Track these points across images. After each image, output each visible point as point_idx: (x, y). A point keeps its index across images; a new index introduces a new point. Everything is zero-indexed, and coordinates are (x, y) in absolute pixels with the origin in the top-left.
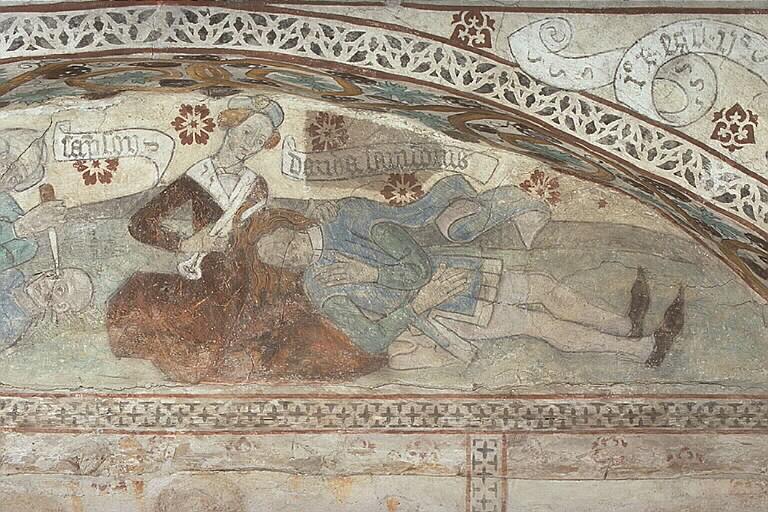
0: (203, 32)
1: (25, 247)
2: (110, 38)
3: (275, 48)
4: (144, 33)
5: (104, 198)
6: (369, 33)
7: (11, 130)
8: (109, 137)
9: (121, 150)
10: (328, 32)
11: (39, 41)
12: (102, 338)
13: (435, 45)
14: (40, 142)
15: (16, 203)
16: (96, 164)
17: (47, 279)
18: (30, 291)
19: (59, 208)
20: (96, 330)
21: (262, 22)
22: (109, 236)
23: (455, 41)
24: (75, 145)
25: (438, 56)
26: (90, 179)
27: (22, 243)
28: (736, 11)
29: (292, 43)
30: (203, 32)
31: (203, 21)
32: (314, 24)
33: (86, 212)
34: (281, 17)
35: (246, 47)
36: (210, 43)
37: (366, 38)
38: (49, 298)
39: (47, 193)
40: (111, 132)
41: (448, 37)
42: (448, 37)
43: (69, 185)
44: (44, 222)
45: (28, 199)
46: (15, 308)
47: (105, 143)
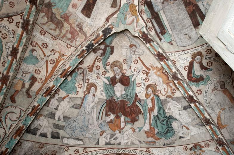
0: (120, 151)
2: (110, 152)
3: (127, 153)
4: (113, 152)
6: (137, 151)
10: (133, 151)
11: (102, 153)
13: (145, 152)
21: (126, 150)
23: (146, 151)
25: (145, 153)
28: (175, 146)
29: (129, 152)
30: (120, 151)
31: (120, 150)
32: (131, 150)
34: (128, 149)
35: (124, 153)
36: (120, 153)
37: (137, 151)
41: (146, 151)
42: (146, 151)
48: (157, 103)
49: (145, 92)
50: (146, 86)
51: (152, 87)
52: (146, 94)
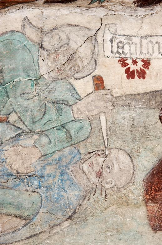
1: (81, 128)
5: (141, 91)
7: (71, 25)
8: (144, 41)
9: (153, 53)
12: (141, 213)
14: (93, 38)
15: (74, 89)
16: (135, 62)
17: (98, 158)
18: (85, 167)
19: (108, 96)
20: (136, 205)
22: (145, 123)
24: (120, 44)
26: (130, 74)
27: (78, 125)
33: (129, 101)
38: (99, 174)
39: (99, 83)
40: (146, 37)
43: (114, 76)
44: (96, 107)
45: (84, 86)
46: (72, 183)
47: (141, 46)
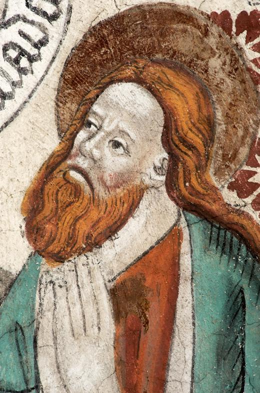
48: (208, 355)
49: (32, 139)
50: (75, 35)
51: (188, 67)
52: (52, 167)
